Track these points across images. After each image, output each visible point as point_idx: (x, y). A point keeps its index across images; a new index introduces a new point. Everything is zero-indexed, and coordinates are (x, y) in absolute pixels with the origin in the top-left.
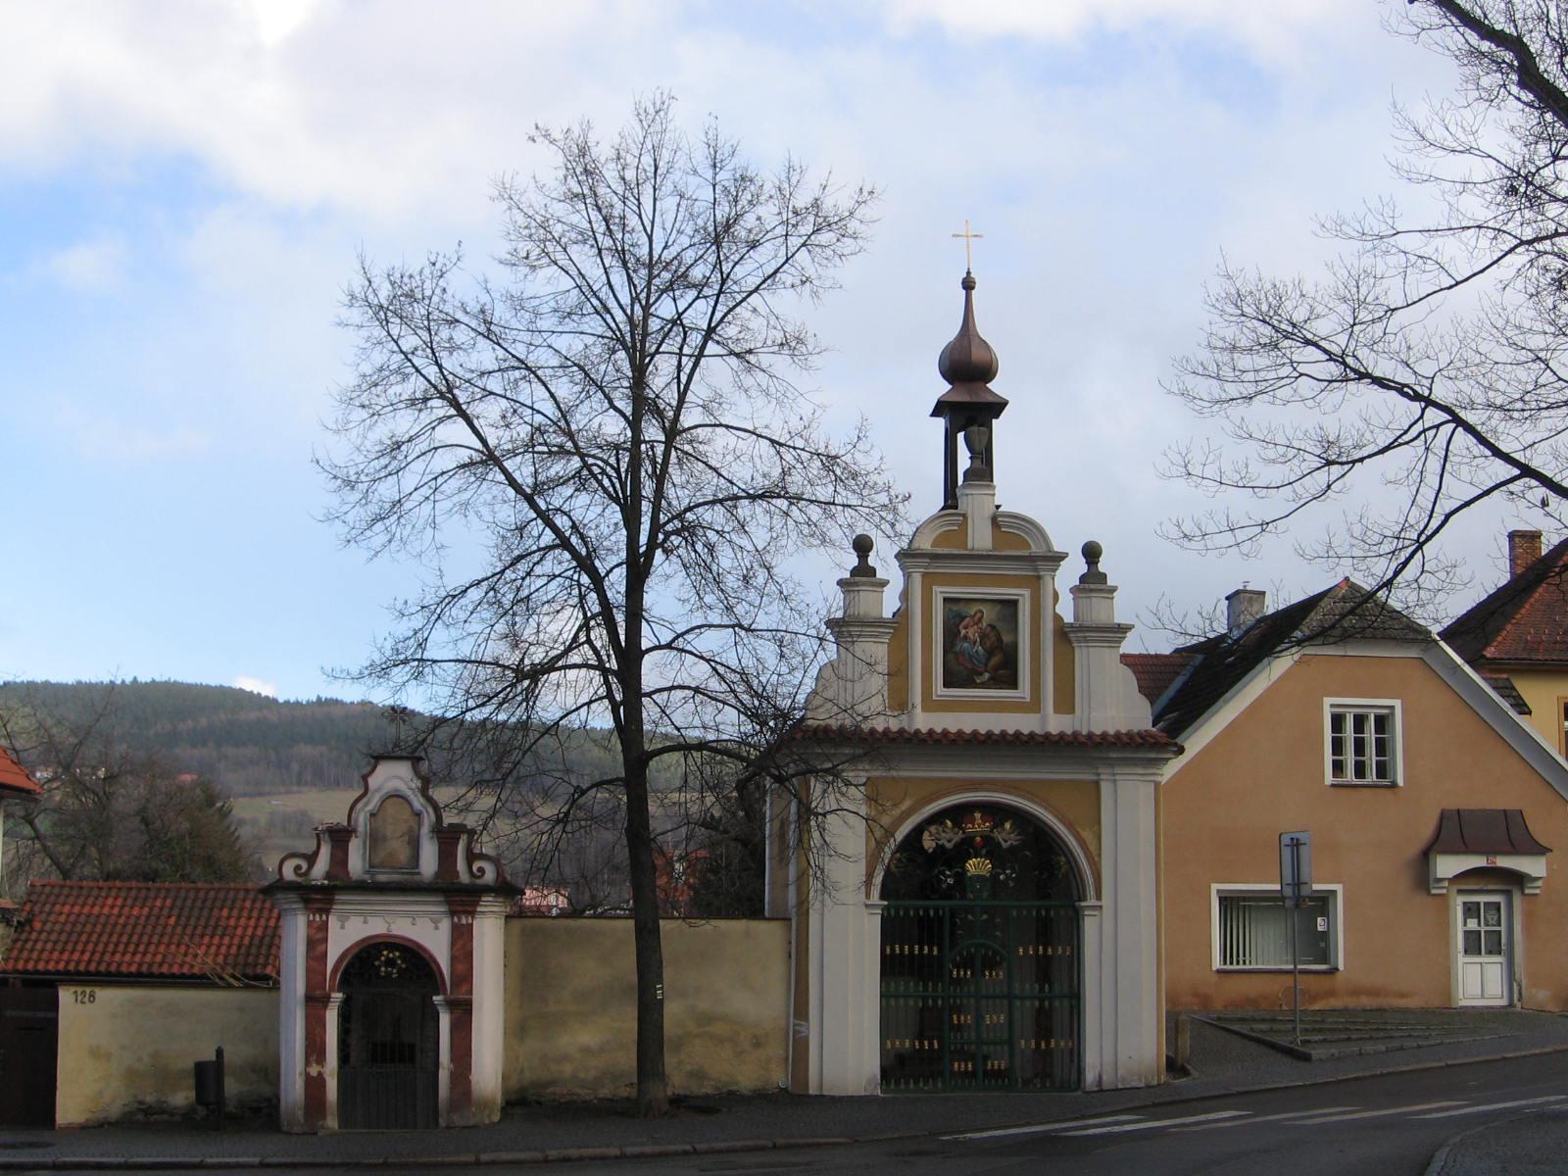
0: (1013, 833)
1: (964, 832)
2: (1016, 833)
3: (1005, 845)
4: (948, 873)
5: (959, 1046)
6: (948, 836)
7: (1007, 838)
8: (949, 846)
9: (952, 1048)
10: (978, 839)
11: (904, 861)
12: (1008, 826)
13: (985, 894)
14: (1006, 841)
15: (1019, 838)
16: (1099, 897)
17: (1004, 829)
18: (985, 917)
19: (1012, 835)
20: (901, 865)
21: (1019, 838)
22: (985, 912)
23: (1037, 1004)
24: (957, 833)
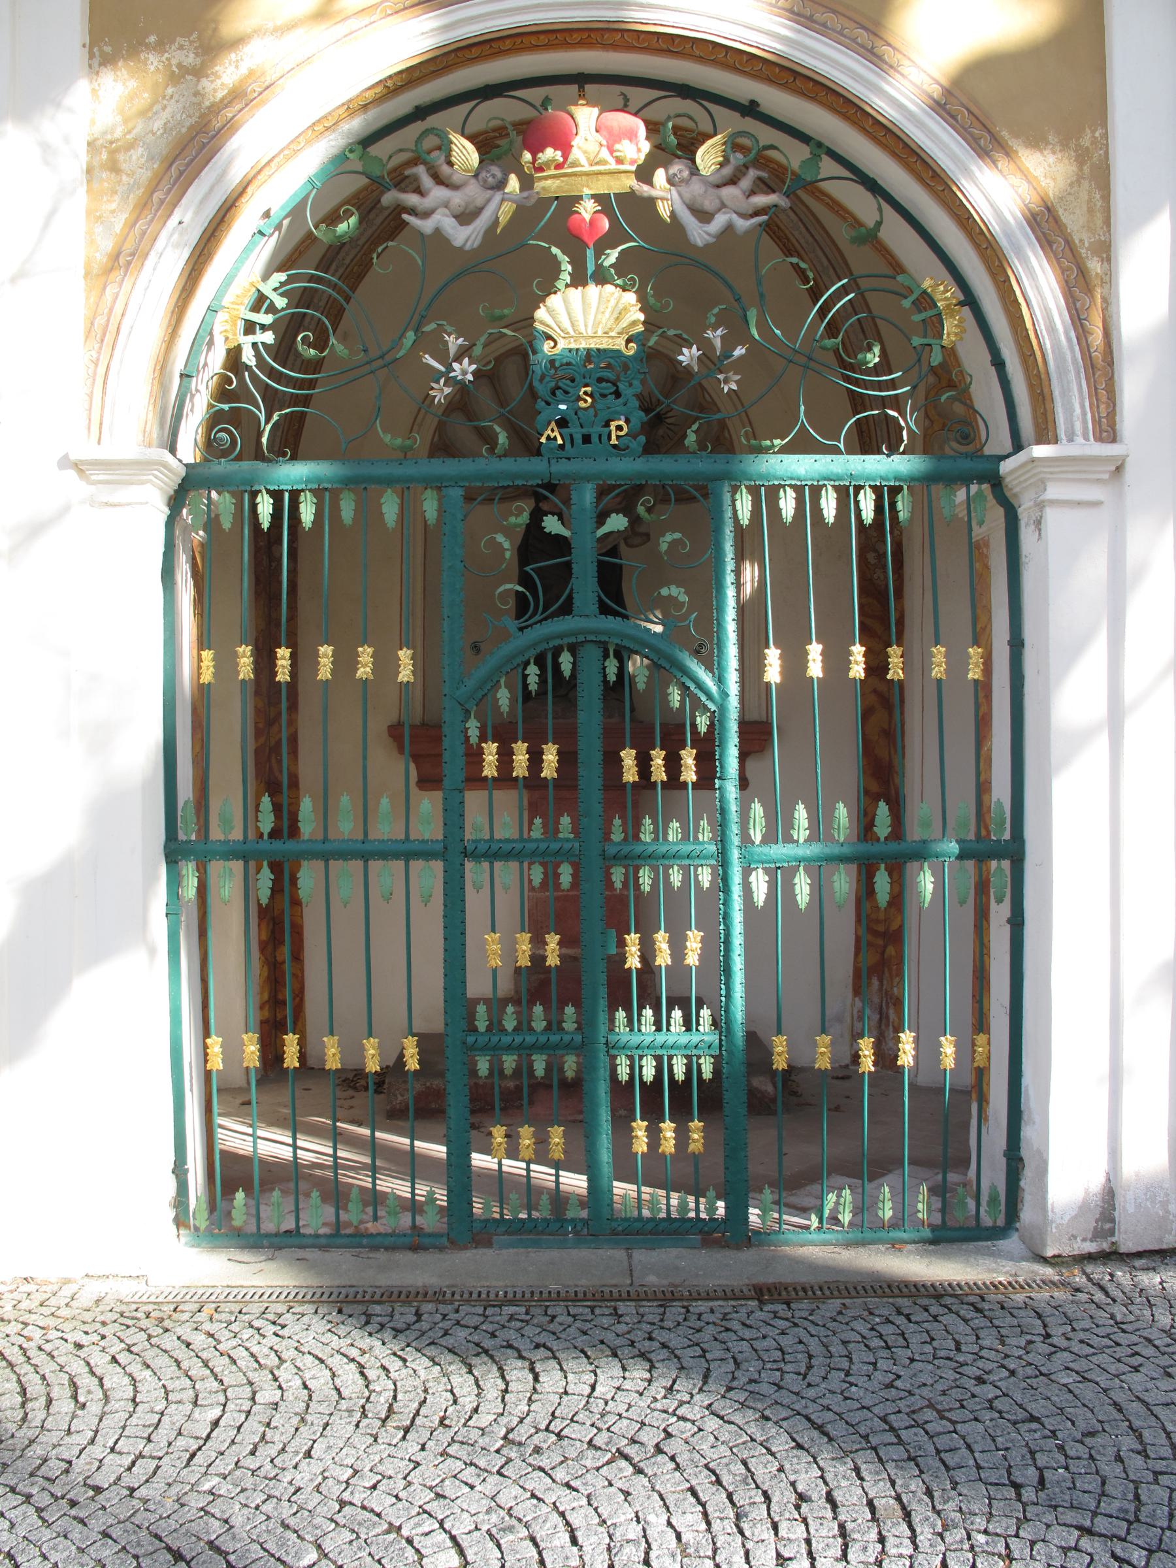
0: (733, 181)
1: (527, 182)
2: (746, 183)
3: (699, 234)
4: (454, 343)
5: (509, 1062)
6: (457, 199)
7: (709, 204)
8: (463, 236)
9: (483, 1066)
10: (587, 209)
11: (281, 302)
12: (708, 157)
13: (619, 428)
14: (704, 216)
15: (761, 200)
16: (1107, 430)
17: (695, 171)
18: (617, 522)
19: (729, 192)
20: (268, 319)
21: (761, 200)
22: (627, 509)
23: (537, 874)
24: (501, 185)
